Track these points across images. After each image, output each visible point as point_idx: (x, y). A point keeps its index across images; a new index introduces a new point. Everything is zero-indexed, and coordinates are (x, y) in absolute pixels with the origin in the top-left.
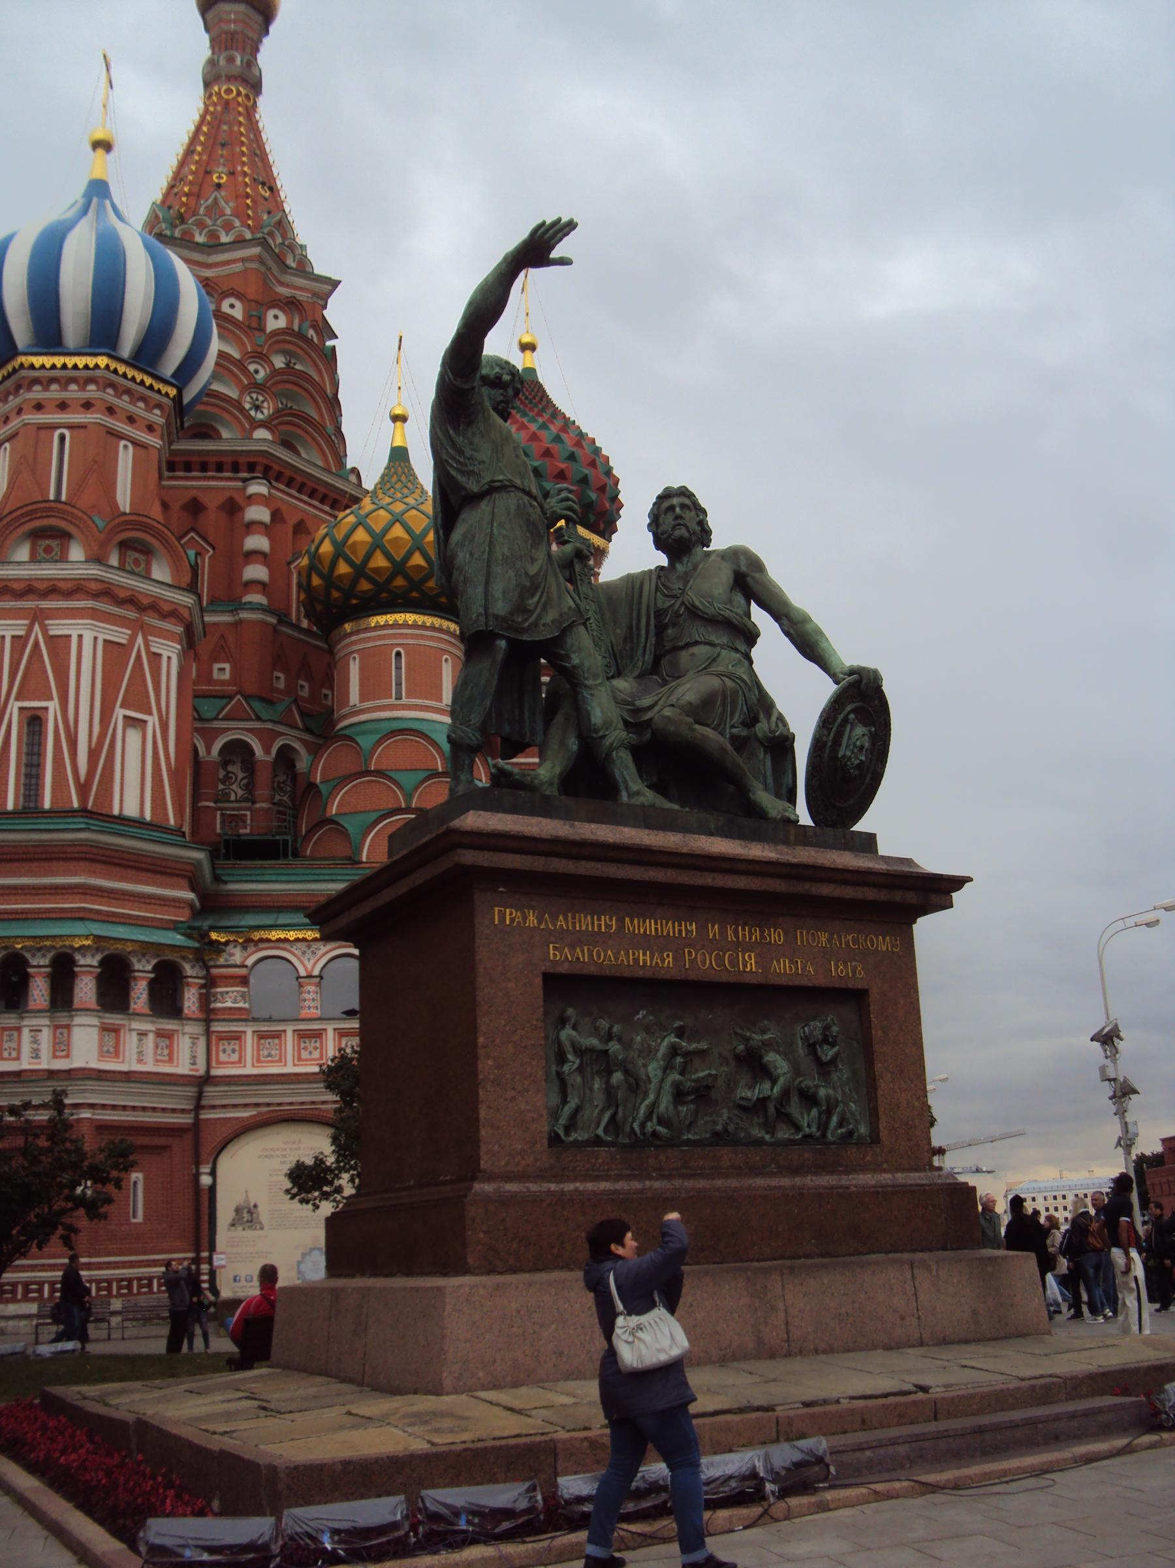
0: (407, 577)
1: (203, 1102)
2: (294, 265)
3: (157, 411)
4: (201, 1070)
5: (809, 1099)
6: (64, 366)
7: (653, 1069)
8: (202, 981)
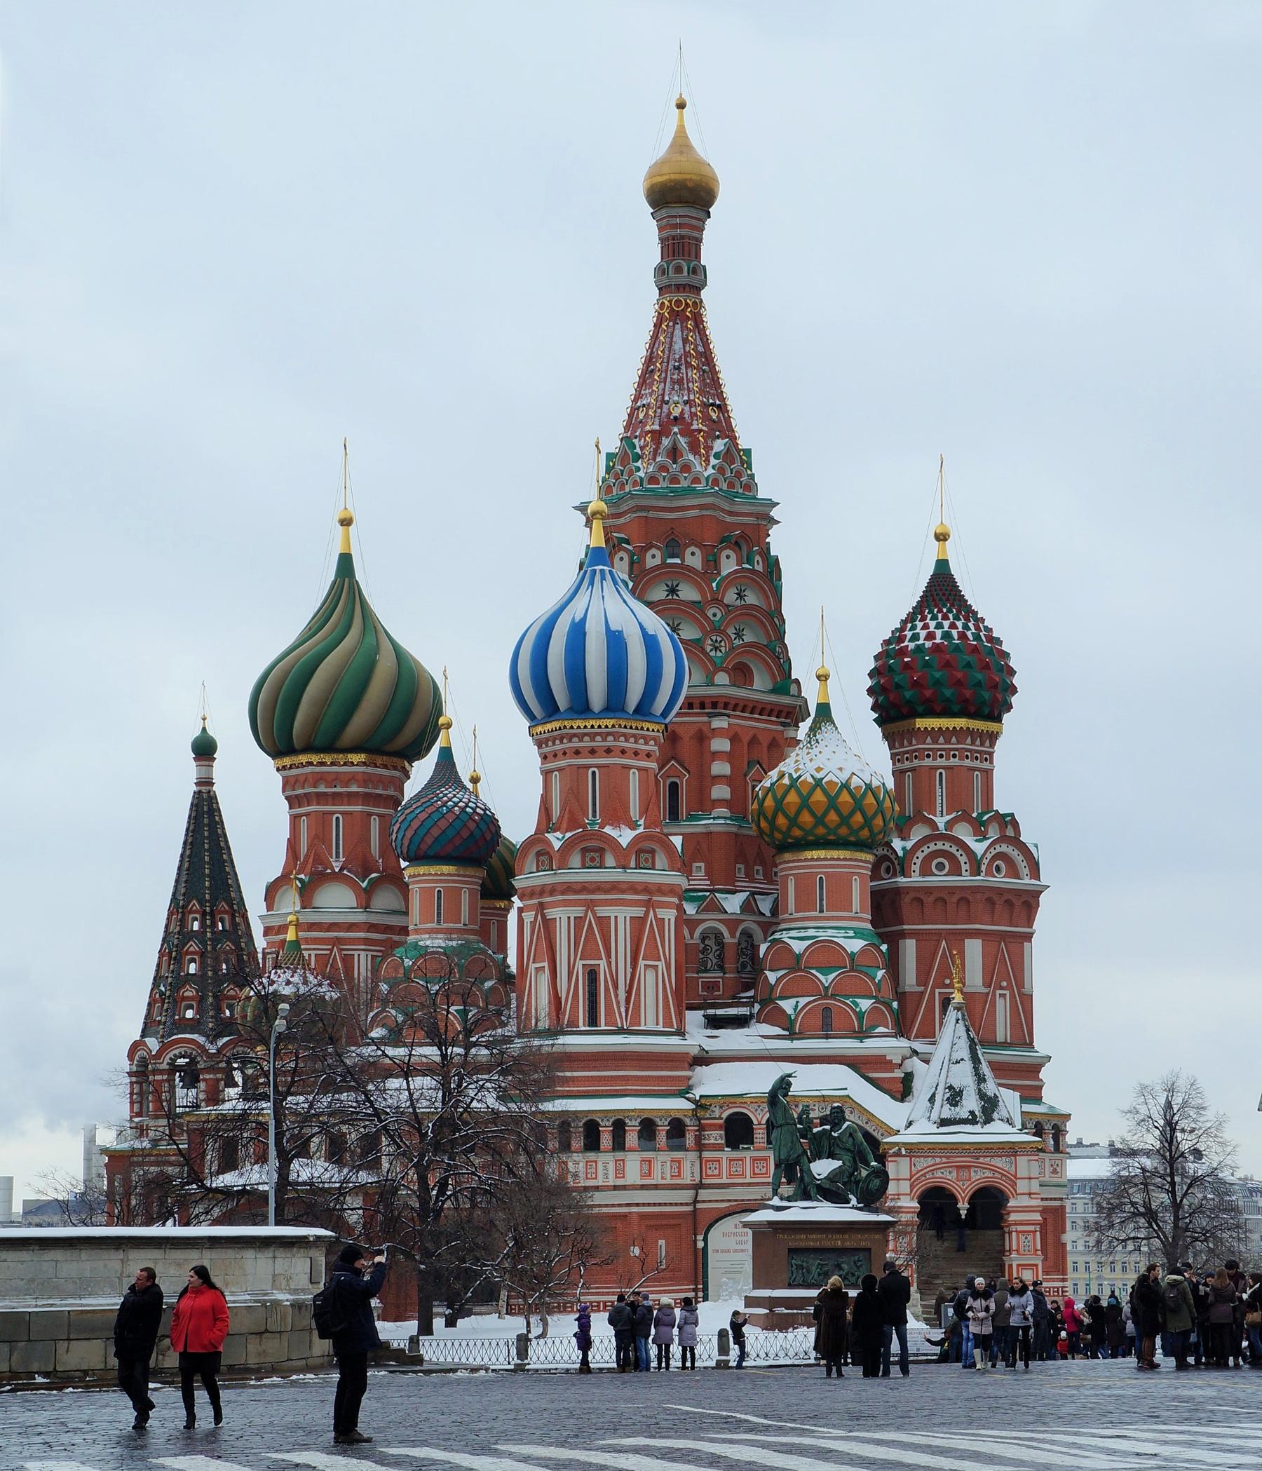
0: (825, 826)
1: (698, 1199)
3: (652, 742)
4: (697, 1181)
5: (853, 1275)
6: (592, 727)
7: (814, 1268)
8: (697, 1128)
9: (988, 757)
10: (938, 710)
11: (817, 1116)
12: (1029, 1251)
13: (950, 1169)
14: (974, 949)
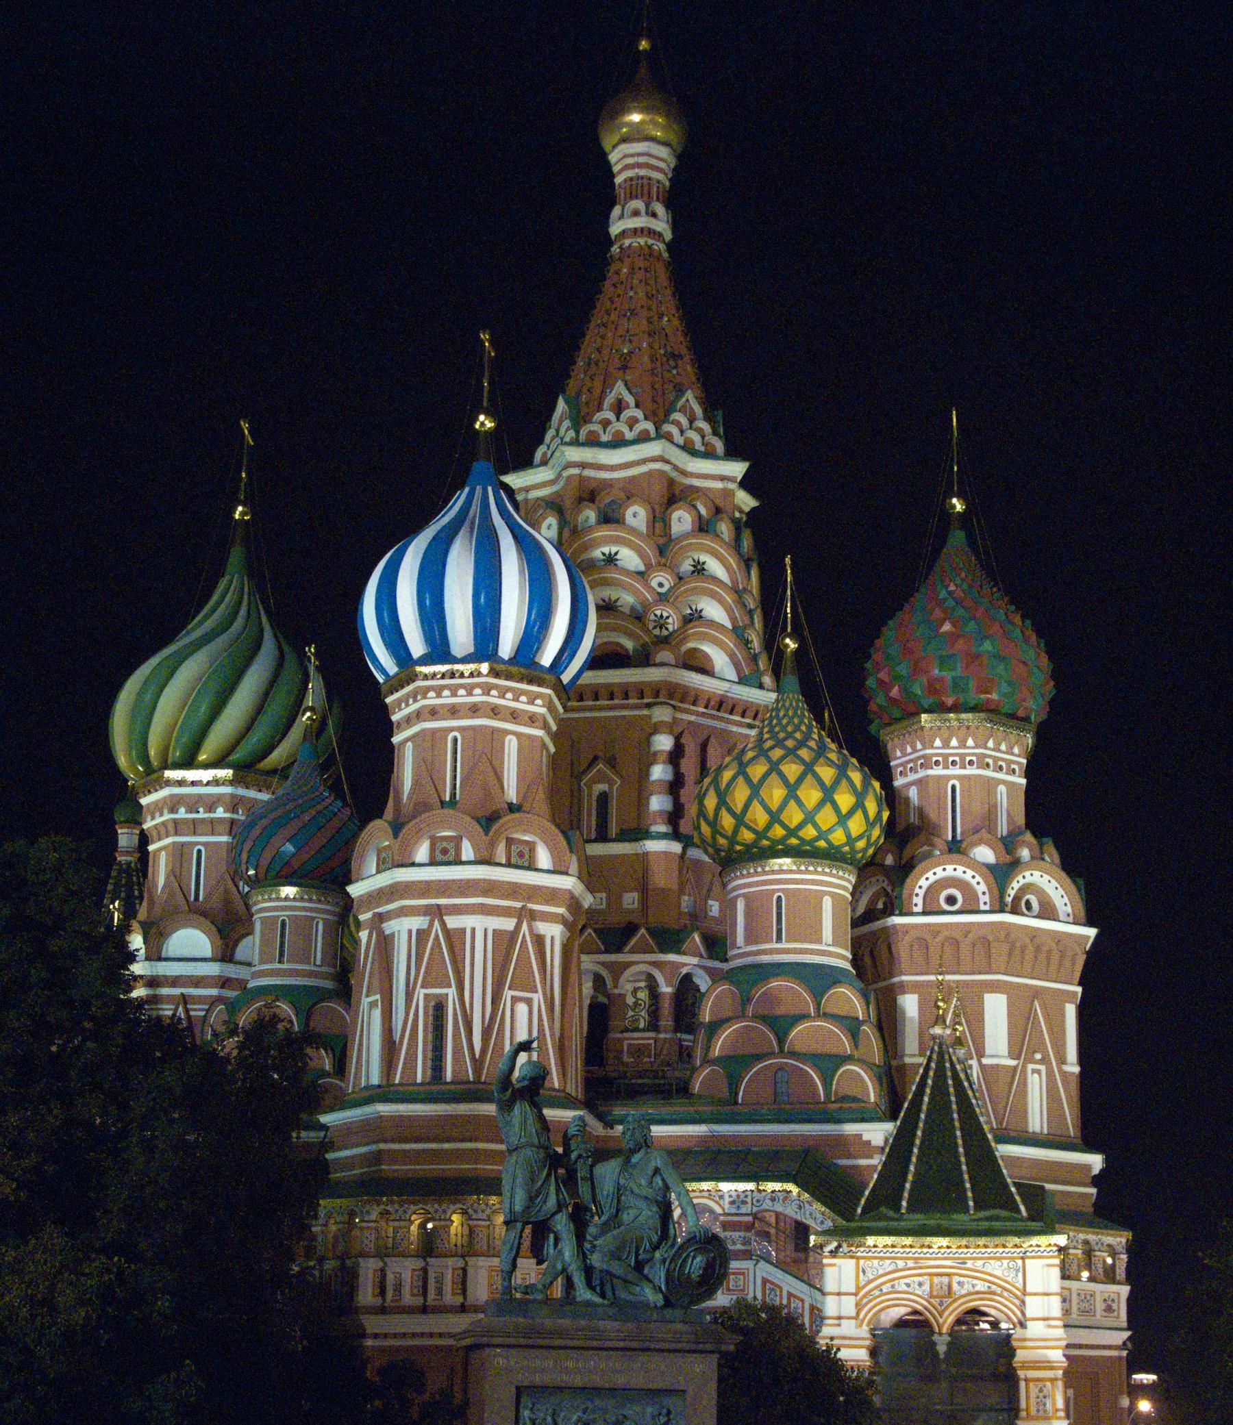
2: (702, 449)
3: (539, 702)
9: (1016, 767)
10: (950, 701)
11: (749, 1212)
12: (1045, 1411)
13: (920, 1279)
14: (996, 1008)
